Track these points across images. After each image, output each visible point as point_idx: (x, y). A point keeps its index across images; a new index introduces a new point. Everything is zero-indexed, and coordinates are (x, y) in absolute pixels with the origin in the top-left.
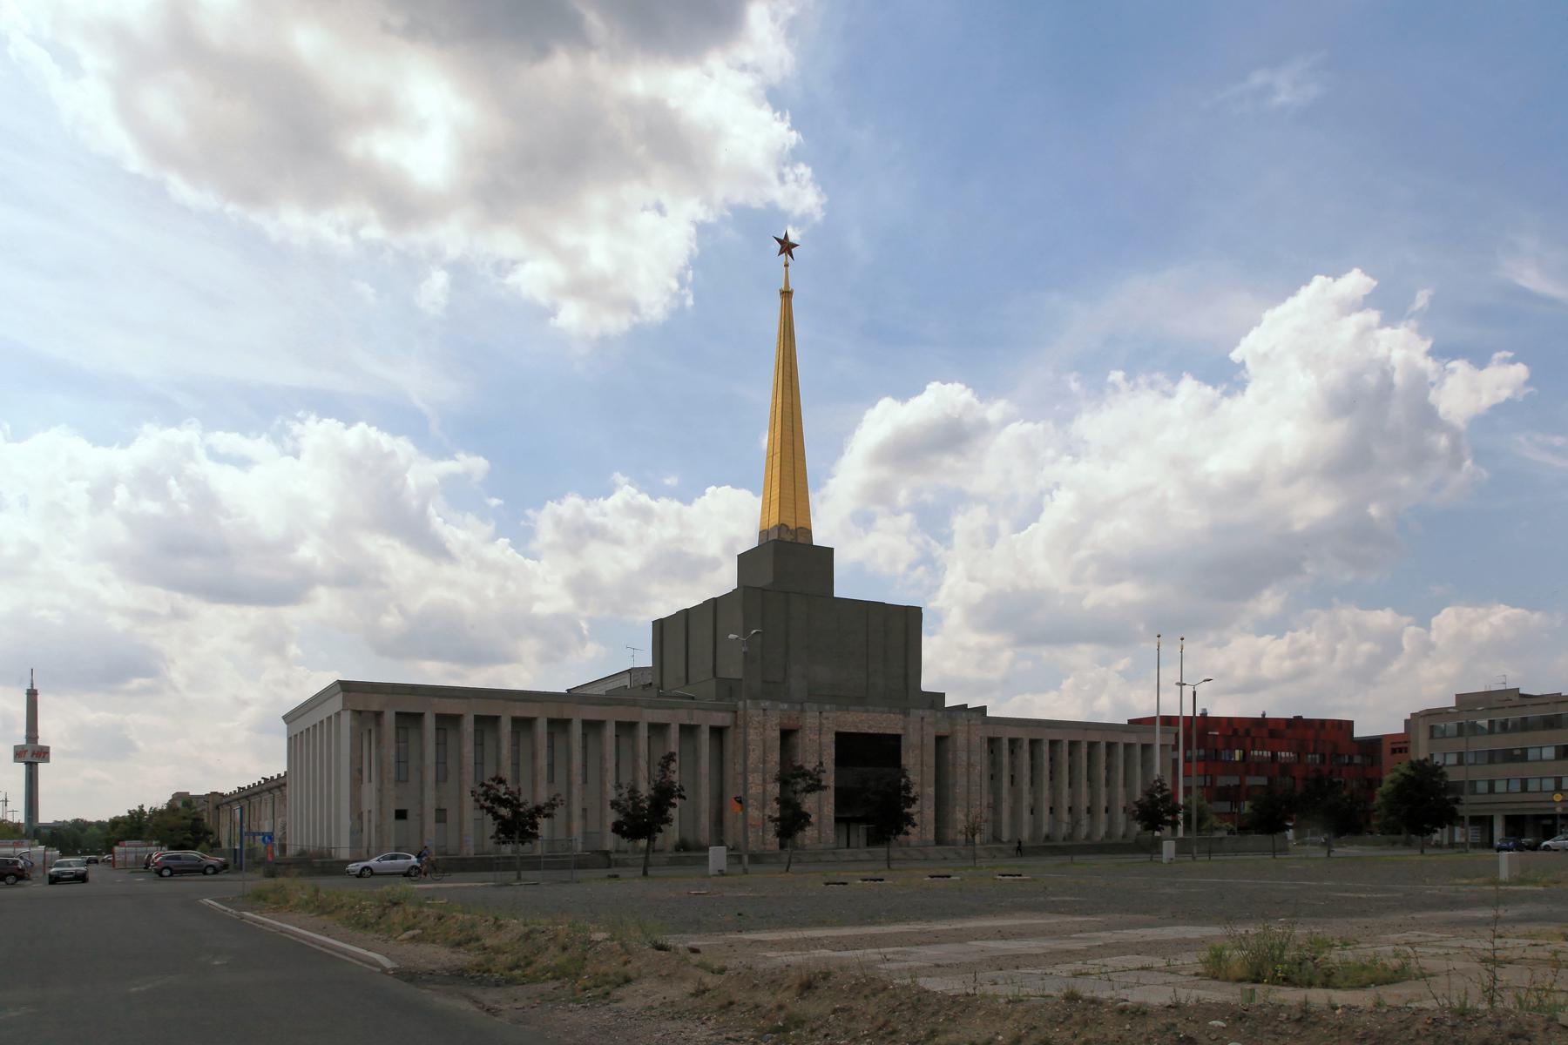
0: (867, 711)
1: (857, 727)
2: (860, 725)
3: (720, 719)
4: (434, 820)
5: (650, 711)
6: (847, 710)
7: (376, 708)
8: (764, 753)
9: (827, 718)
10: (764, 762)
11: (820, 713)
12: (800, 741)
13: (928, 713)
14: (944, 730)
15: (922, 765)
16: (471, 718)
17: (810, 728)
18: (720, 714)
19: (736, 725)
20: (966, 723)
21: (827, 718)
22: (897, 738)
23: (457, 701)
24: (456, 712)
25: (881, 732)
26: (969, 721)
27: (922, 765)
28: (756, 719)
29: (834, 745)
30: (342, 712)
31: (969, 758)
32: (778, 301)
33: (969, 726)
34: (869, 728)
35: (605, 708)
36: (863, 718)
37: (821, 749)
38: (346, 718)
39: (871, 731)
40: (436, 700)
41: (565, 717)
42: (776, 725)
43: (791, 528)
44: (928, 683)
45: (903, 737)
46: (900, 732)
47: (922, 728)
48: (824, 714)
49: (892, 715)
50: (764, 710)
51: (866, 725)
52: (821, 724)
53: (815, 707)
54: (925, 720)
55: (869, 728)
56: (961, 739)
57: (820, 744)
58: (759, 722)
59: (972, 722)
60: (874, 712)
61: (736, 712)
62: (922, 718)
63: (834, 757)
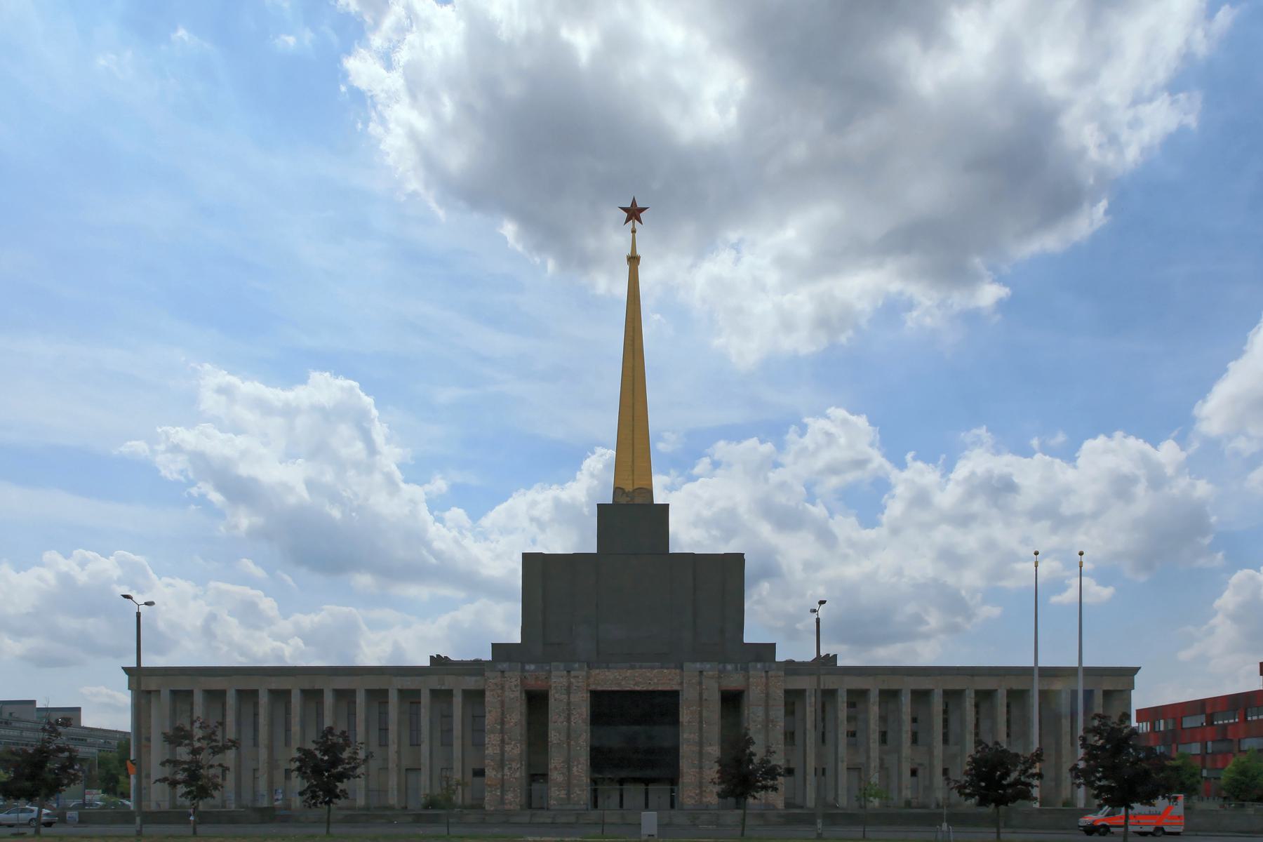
0: (632, 668)
2: (623, 683)
5: (398, 678)
6: (608, 668)
8: (503, 713)
9: (575, 677)
10: (502, 723)
13: (708, 666)
14: (734, 682)
15: (701, 722)
20: (764, 674)
21: (575, 677)
22: (675, 694)
25: (651, 688)
26: (767, 672)
27: (701, 722)
32: (625, 269)
33: (767, 678)
34: (634, 685)
37: (569, 710)
39: (637, 688)
41: (317, 687)
44: (753, 634)
46: (676, 688)
47: (700, 683)
48: (573, 673)
50: (503, 672)
53: (562, 666)
54: (705, 673)
55: (634, 685)
56: (754, 694)
57: (569, 704)
58: (496, 684)
59: (770, 673)
60: (641, 667)
62: (701, 672)
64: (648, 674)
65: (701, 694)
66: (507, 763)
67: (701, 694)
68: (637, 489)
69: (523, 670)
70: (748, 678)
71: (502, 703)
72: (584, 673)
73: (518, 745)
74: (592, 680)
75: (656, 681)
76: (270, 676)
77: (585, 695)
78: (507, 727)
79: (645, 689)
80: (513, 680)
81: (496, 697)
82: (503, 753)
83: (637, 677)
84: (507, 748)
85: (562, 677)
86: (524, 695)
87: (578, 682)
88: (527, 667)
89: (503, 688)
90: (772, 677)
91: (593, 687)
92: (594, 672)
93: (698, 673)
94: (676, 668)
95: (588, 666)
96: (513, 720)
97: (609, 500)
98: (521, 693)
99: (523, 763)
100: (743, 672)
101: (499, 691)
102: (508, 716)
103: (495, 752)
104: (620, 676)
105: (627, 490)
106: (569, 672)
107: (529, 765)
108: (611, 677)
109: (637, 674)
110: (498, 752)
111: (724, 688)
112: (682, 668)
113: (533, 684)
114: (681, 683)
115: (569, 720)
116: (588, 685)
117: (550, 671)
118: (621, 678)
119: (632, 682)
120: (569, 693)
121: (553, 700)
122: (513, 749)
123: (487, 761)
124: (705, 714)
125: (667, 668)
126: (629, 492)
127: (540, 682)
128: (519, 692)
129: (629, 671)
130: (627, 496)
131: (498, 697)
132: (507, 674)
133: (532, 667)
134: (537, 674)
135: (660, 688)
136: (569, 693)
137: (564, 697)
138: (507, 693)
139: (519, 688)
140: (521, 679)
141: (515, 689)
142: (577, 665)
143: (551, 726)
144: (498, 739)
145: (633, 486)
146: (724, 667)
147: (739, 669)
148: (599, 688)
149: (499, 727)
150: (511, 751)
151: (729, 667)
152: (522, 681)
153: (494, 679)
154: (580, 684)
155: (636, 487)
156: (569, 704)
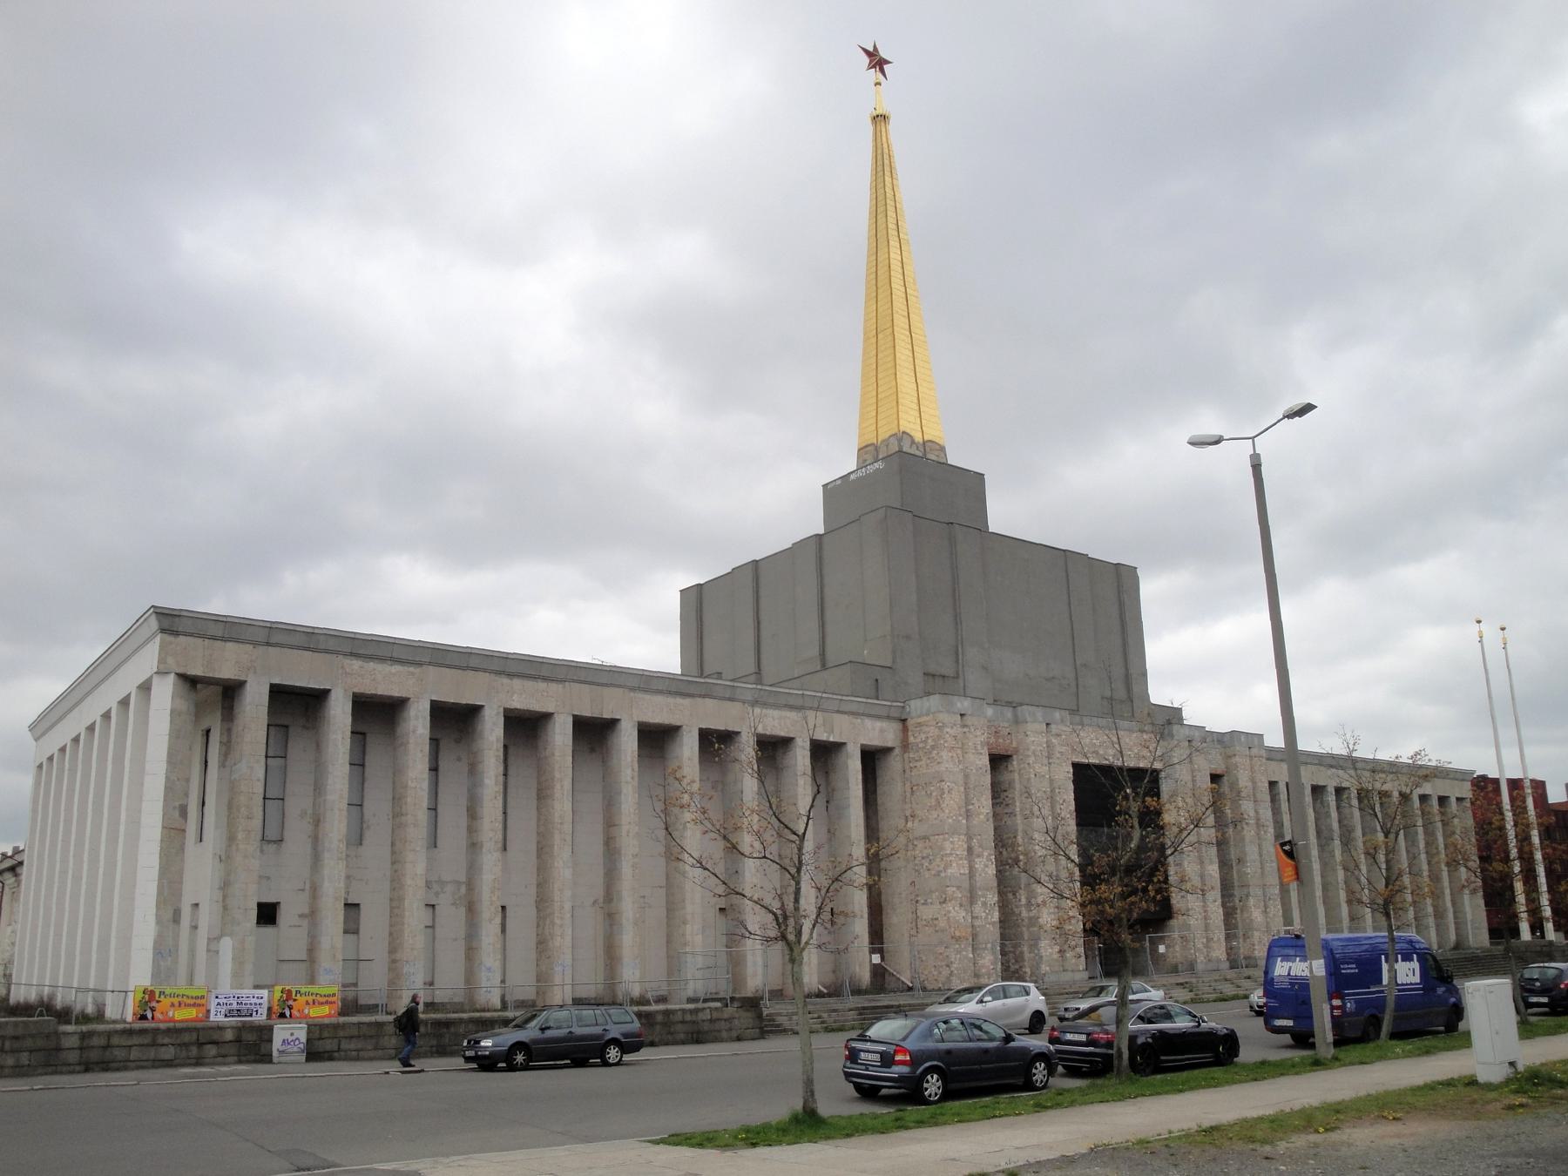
3: (878, 733)
4: (342, 931)
7: (227, 672)
8: (967, 795)
11: (1047, 724)
12: (1016, 776)
16: (425, 707)
18: (879, 724)
19: (905, 746)
23: (396, 668)
24: (396, 692)
28: (948, 730)
29: (1071, 787)
30: (156, 680)
35: (679, 700)
37: (1052, 791)
38: (165, 693)
40: (356, 664)
41: (606, 715)
43: (916, 440)
52: (1049, 745)
53: (1039, 713)
57: (1051, 781)
61: (904, 721)
63: (1073, 807)
71: (966, 776)
76: (511, 675)
102: (975, 801)
104: (1097, 739)
127: (1001, 740)
132: (969, 720)
134: (996, 723)
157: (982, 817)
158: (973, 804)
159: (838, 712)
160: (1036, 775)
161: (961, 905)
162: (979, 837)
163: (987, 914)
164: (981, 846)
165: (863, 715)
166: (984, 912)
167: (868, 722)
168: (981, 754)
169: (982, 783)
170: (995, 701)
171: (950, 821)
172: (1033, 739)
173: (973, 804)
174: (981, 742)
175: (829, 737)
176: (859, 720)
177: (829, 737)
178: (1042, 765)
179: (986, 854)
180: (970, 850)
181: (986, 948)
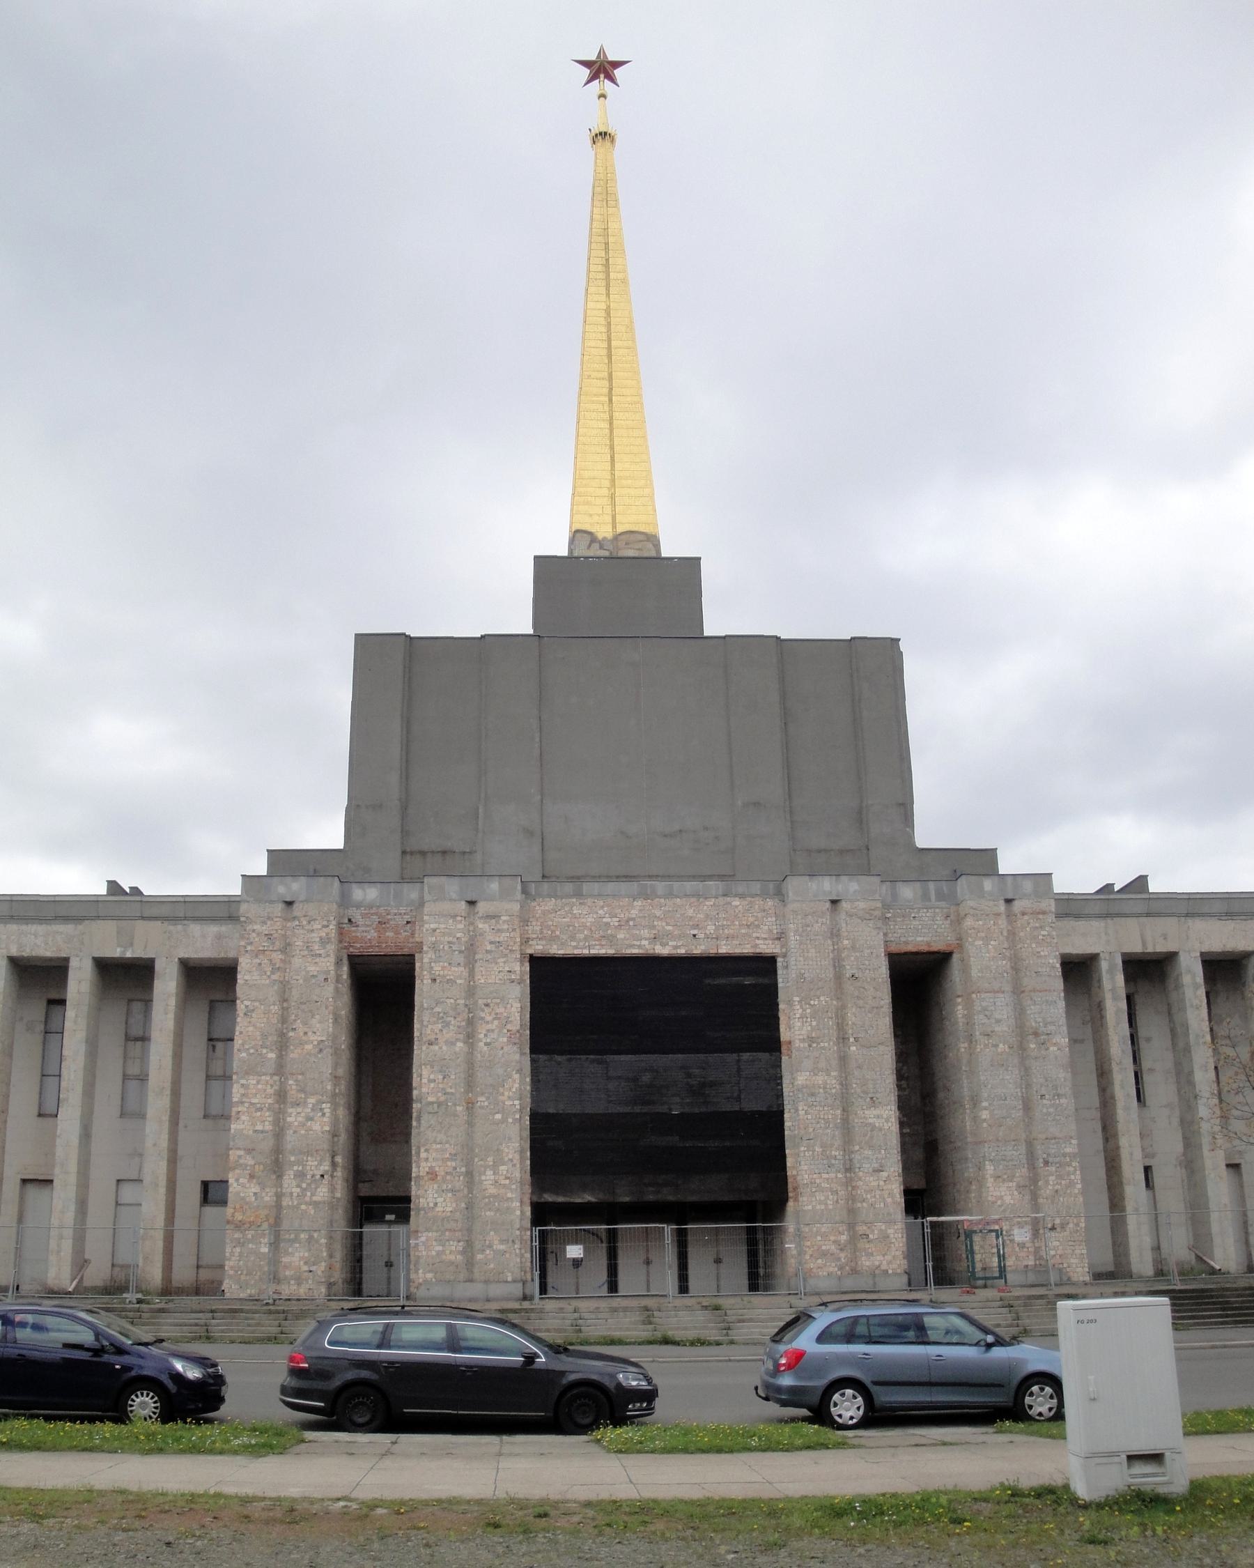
1: (611, 939)
2: (621, 936)
6: (578, 894)
8: (284, 1020)
10: (282, 1044)
15: (842, 1039)
17: (434, 947)
18: (213, 929)
20: (1002, 907)
21: (489, 917)
22: (765, 966)
25: (698, 949)
27: (842, 1039)
28: (257, 927)
31: (1020, 1013)
33: (1010, 916)
36: (634, 913)
42: (324, 942)
45: (779, 960)
46: (766, 948)
47: (835, 934)
48: (482, 907)
49: (736, 902)
51: (645, 933)
53: (452, 887)
54: (845, 905)
57: (471, 991)
58: (269, 936)
59: (1018, 906)
60: (670, 895)
64: (690, 912)
65: (838, 964)
66: (293, 1159)
67: (838, 964)
68: (620, 535)
69: (345, 900)
70: (959, 920)
71: (284, 987)
72: (516, 907)
73: (327, 1107)
74: (534, 928)
75: (711, 929)
77: (517, 967)
78: (294, 1054)
79: (682, 951)
80: (317, 926)
81: (268, 969)
82: (279, 1132)
83: (659, 919)
84: (294, 1117)
85: (454, 917)
86: (345, 968)
87: (499, 931)
88: (358, 893)
89: (286, 948)
90: (1023, 914)
91: (538, 948)
92: (543, 906)
93: (828, 905)
94: (764, 894)
95: (525, 891)
96: (312, 1037)
97: (560, 549)
98: (338, 963)
99: (339, 1159)
100: (943, 904)
101: (277, 957)
102: (298, 1024)
103: (259, 1127)
104: (613, 916)
105: (600, 536)
106: (472, 903)
107: (358, 1174)
108: (590, 920)
109: (658, 913)
110: (268, 1127)
111: (894, 948)
112: (780, 894)
113: (370, 939)
114: (780, 937)
115: (470, 1038)
116: (526, 941)
117: (422, 904)
118: (615, 922)
119: (645, 933)
120: (470, 964)
121: (427, 981)
122: (311, 1119)
123: (233, 1155)
124: (852, 1016)
125: (742, 896)
126: (605, 539)
127: (390, 934)
128: (332, 959)
129: (638, 903)
130: (601, 547)
131: (273, 973)
132: (297, 910)
133: (372, 893)
135: (724, 949)
136: (470, 964)
137: (458, 972)
138: (297, 962)
139: (332, 948)
140: (339, 924)
141: (322, 952)
142: (494, 886)
143: (421, 1052)
144: (270, 1091)
145: (614, 526)
146: (895, 896)
147: (933, 897)
148: (556, 950)
149: (272, 1055)
150: (303, 1125)
151: (907, 892)
152: (341, 932)
153: (264, 923)
154: (503, 937)
155: (620, 529)
156: (471, 991)
157: (309, 1047)
158: (294, 1029)
159: (143, 918)
160: (434, 980)
161: (252, 1176)
162: (300, 1077)
163: (304, 1190)
164: (302, 1090)
165: (185, 918)
166: (298, 1186)
167: (195, 929)
168: (320, 955)
169: (315, 998)
170: (544, 876)
171: (244, 1055)
172: (433, 926)
173: (294, 1029)
174: (321, 938)
175: (124, 952)
176: (180, 927)
177: (124, 952)
178: (450, 964)
179: (312, 1100)
180: (281, 1096)
181: (296, 1240)
